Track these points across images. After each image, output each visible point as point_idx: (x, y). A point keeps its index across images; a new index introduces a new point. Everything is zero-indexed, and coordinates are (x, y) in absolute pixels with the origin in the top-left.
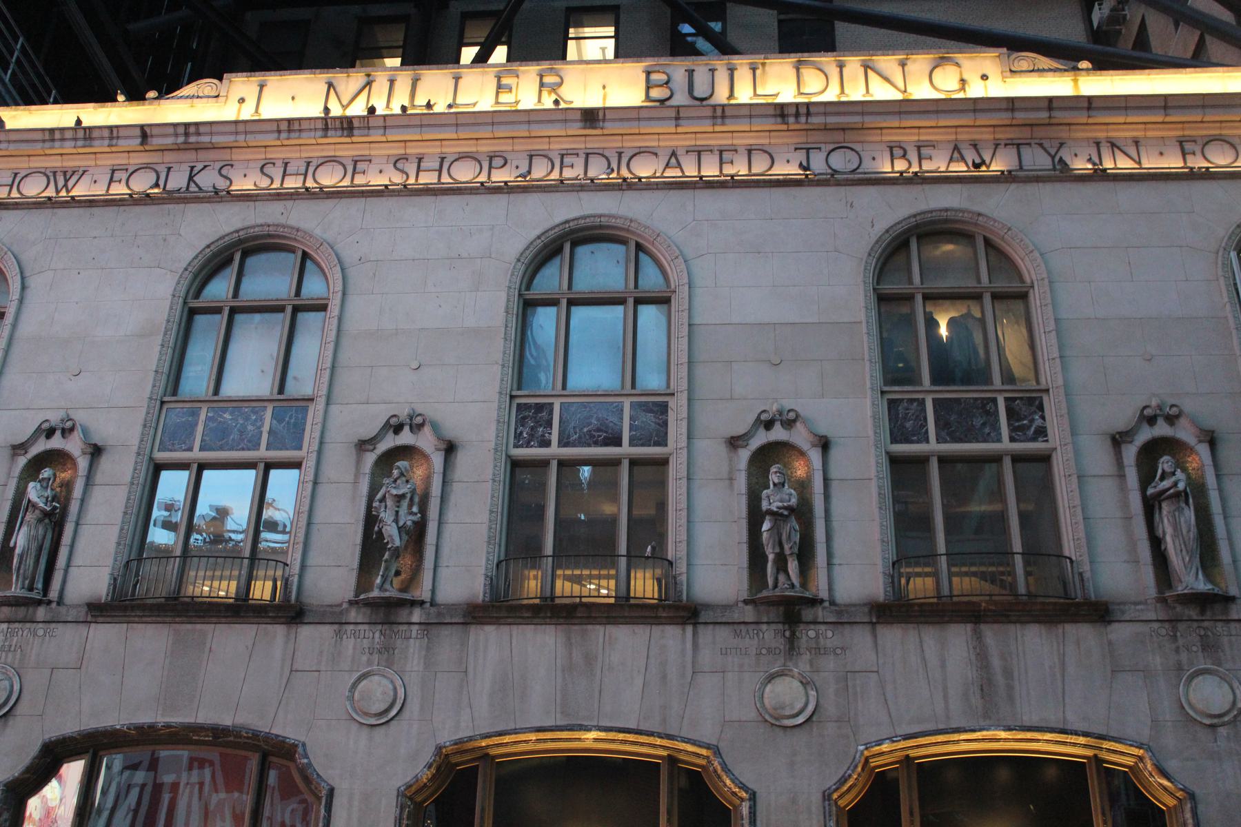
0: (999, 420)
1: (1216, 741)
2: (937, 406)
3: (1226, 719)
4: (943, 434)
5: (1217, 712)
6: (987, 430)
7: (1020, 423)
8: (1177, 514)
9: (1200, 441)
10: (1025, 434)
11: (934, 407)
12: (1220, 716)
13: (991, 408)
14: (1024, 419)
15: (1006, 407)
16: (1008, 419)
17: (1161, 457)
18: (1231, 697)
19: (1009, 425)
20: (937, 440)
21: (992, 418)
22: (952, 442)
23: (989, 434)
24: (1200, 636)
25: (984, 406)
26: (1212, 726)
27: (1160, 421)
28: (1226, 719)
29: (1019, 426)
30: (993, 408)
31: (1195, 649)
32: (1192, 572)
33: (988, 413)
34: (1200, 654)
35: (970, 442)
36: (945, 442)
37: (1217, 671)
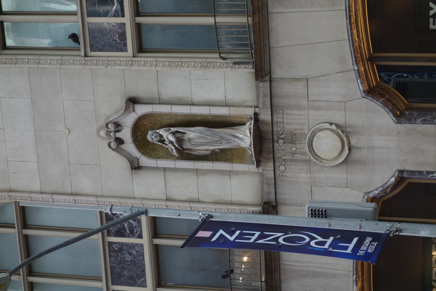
0: (126, 243)
1: (360, 148)
2: (118, 283)
3: (345, 139)
4: (139, 282)
5: (340, 144)
6: (135, 253)
7: (127, 229)
8: (193, 143)
9: (134, 111)
10: (135, 227)
11: (119, 285)
12: (342, 141)
13: (117, 247)
14: (124, 226)
15: (115, 236)
16: (125, 236)
17: (148, 140)
18: (328, 132)
19: (129, 237)
20: (144, 287)
21: (125, 248)
22: (145, 277)
23: (137, 252)
24: (284, 143)
25: (115, 251)
26: (350, 149)
27: (118, 135)
28: (345, 139)
29: (130, 230)
30: (117, 245)
31: (294, 149)
32: (237, 141)
33: (121, 250)
34: (298, 146)
35: (144, 264)
36: (145, 281)
37: (310, 137)
